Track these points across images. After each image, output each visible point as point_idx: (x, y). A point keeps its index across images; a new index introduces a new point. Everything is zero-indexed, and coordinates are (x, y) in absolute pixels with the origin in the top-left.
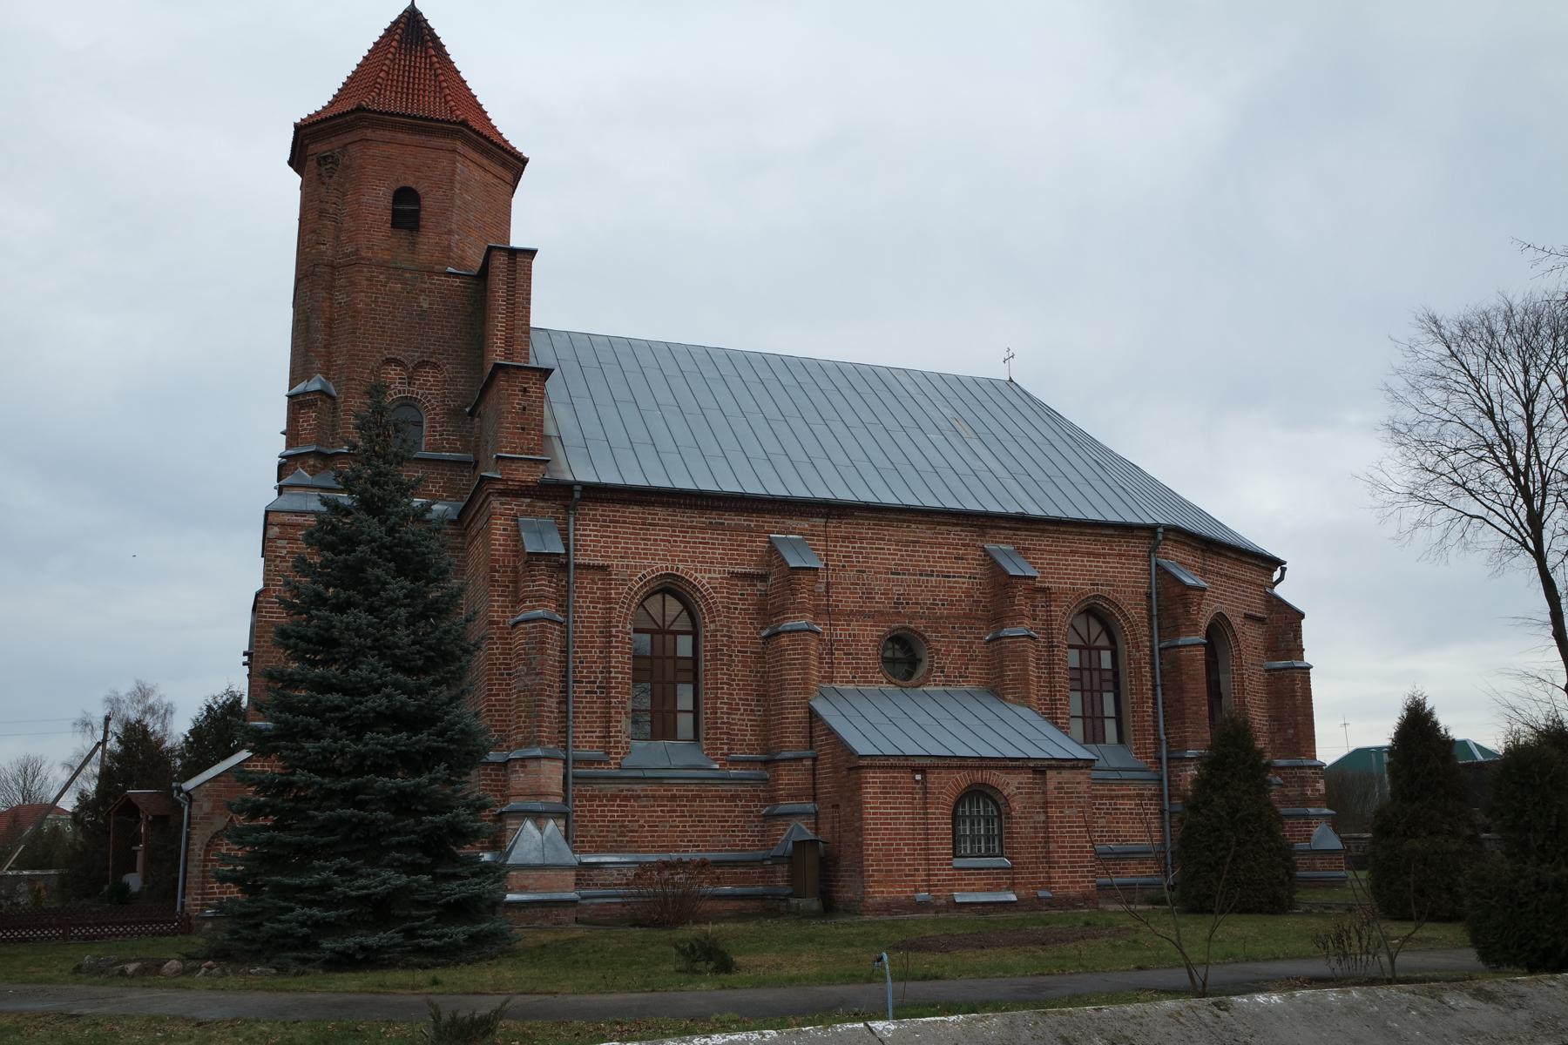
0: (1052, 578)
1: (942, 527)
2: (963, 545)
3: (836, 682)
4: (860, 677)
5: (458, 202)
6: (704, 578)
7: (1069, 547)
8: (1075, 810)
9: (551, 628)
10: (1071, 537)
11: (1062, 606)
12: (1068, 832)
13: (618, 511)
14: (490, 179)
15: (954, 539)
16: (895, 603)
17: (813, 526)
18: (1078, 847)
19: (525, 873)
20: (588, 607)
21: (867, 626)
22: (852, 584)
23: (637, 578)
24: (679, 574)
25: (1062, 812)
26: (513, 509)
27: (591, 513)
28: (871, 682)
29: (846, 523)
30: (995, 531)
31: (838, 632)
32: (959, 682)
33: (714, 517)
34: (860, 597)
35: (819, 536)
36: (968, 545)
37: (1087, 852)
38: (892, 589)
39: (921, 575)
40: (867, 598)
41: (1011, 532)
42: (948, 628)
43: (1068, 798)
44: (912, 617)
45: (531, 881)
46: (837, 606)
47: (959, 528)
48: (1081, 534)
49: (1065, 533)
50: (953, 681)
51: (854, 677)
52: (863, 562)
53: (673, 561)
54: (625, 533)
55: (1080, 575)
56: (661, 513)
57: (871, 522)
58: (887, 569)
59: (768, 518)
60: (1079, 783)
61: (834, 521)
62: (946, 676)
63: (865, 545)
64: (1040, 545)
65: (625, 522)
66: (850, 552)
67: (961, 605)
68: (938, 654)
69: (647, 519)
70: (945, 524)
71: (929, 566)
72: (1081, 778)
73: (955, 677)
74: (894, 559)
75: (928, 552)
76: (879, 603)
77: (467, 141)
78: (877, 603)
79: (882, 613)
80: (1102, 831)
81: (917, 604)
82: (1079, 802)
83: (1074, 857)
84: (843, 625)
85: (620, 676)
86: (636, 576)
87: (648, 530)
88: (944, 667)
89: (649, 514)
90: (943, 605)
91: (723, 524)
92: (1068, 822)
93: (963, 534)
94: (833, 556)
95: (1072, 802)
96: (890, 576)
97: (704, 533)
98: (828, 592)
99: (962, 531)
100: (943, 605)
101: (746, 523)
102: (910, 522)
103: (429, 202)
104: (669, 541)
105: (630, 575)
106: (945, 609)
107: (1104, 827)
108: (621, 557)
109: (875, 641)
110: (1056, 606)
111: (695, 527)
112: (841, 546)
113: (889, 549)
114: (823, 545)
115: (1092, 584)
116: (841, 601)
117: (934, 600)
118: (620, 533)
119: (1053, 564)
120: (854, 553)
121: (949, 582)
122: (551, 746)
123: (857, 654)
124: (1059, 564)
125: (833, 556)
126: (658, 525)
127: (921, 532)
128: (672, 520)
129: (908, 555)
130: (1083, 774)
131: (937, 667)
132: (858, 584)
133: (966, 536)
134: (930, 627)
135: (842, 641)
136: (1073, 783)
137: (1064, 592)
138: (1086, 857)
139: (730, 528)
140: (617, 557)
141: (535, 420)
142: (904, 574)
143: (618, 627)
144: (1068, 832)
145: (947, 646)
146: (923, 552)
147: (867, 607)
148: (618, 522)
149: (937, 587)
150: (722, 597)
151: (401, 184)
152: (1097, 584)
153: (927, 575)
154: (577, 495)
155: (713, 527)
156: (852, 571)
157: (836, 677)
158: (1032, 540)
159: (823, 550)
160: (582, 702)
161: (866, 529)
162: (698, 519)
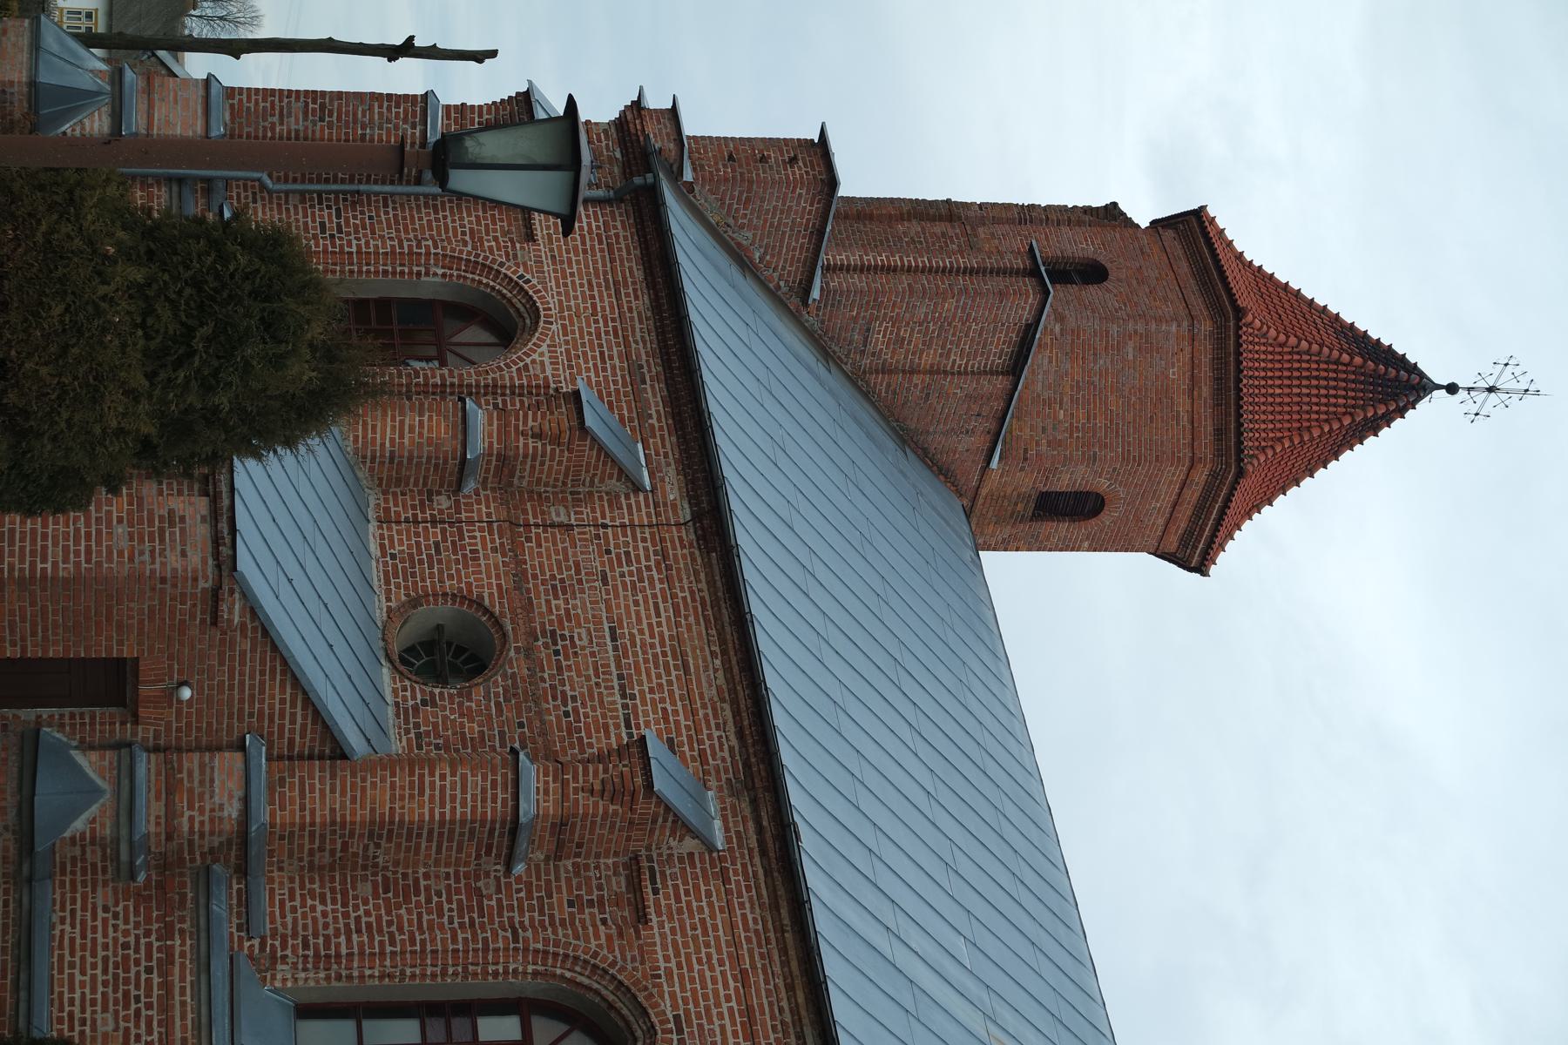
0: (673, 930)
1: (728, 713)
2: (702, 753)
3: (380, 527)
4: (395, 567)
5: (1114, 329)
6: (542, 354)
7: (753, 967)
8: (124, 544)
9: (414, 112)
10: (778, 969)
11: (611, 950)
12: (77, 530)
13: (629, 253)
14: (1182, 405)
15: (710, 737)
16: (553, 633)
17: (674, 506)
18: (44, 548)
19: (27, 35)
20: (462, 226)
21: (498, 577)
22: (577, 564)
23: (521, 271)
24: (541, 324)
25: (120, 520)
26: (599, 140)
27: (619, 224)
28: (387, 582)
29: (692, 554)
30: (747, 812)
31: (478, 534)
32: (407, 732)
33: (652, 368)
34: (553, 577)
35: (658, 514)
36: (704, 762)
37: (33, 565)
38: (579, 626)
39: (620, 677)
40: (554, 587)
41: (754, 844)
42: (519, 715)
43: (151, 534)
44: (528, 652)
45: (13, 39)
46: (529, 540)
47: (734, 742)
48: (790, 988)
49: (784, 951)
50: (407, 722)
51: (393, 557)
52: (624, 584)
53: (562, 318)
54: (596, 262)
55: (694, 991)
56: (642, 303)
57: (706, 594)
58: (620, 620)
59: (671, 441)
60: (184, 554)
61: (693, 537)
62: (416, 709)
63: (658, 586)
64: (742, 905)
65: (612, 261)
66: (638, 562)
67: (572, 746)
68: (460, 695)
69: (626, 286)
70: (736, 714)
71: (642, 692)
72: (195, 559)
73: (417, 725)
74: (641, 632)
75: (671, 693)
76: (549, 608)
77: (1219, 339)
78: (548, 602)
79: (529, 606)
80: (83, 1022)
81: (559, 668)
82: (142, 553)
83: (22, 540)
84: (493, 541)
85: (354, 249)
86: (526, 270)
87: (608, 288)
88: (434, 704)
89: (635, 290)
90: (567, 714)
91: (644, 382)
92: (99, 532)
93: (726, 754)
94: (625, 535)
95: (141, 540)
96: (606, 626)
97: (620, 356)
98: (552, 525)
99: (731, 749)
100: (567, 714)
101: (653, 412)
102: (724, 652)
103: (1093, 292)
104: (594, 313)
105: (525, 264)
106: (557, 717)
107: (94, 1029)
108: (553, 257)
109: (470, 591)
110: (609, 938)
111: (627, 345)
112: (646, 549)
113: (659, 624)
114: (640, 517)
115: (676, 1018)
116: (539, 546)
117: (574, 698)
118: (594, 255)
119: (705, 933)
120: (639, 570)
121: (617, 726)
122: (227, 117)
123: (440, 561)
124: (707, 945)
125: (625, 535)
126: (618, 298)
127: (710, 679)
128: (632, 319)
129: (655, 656)
130: (204, 562)
131: (432, 693)
132: (578, 572)
133: (723, 759)
134: (515, 685)
135: (462, 538)
136: (183, 543)
137: (644, 954)
138: (22, 561)
139: (637, 395)
140: (552, 250)
141: (750, 172)
142: (615, 649)
143: (436, 247)
144: (77, 530)
145: (480, 713)
146: (670, 683)
147: (536, 586)
148: (611, 252)
149: (601, 702)
150: (511, 378)
151: (1108, 266)
152: (680, 1031)
153: (622, 688)
154: (638, 180)
155: (634, 371)
156: (603, 564)
157: (389, 529)
158: (748, 888)
159: (631, 521)
160: (305, 216)
161: (690, 585)
162: (643, 349)
